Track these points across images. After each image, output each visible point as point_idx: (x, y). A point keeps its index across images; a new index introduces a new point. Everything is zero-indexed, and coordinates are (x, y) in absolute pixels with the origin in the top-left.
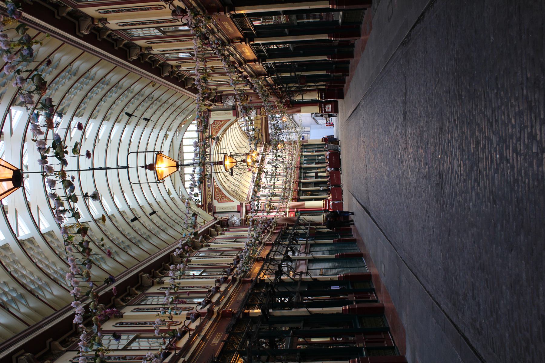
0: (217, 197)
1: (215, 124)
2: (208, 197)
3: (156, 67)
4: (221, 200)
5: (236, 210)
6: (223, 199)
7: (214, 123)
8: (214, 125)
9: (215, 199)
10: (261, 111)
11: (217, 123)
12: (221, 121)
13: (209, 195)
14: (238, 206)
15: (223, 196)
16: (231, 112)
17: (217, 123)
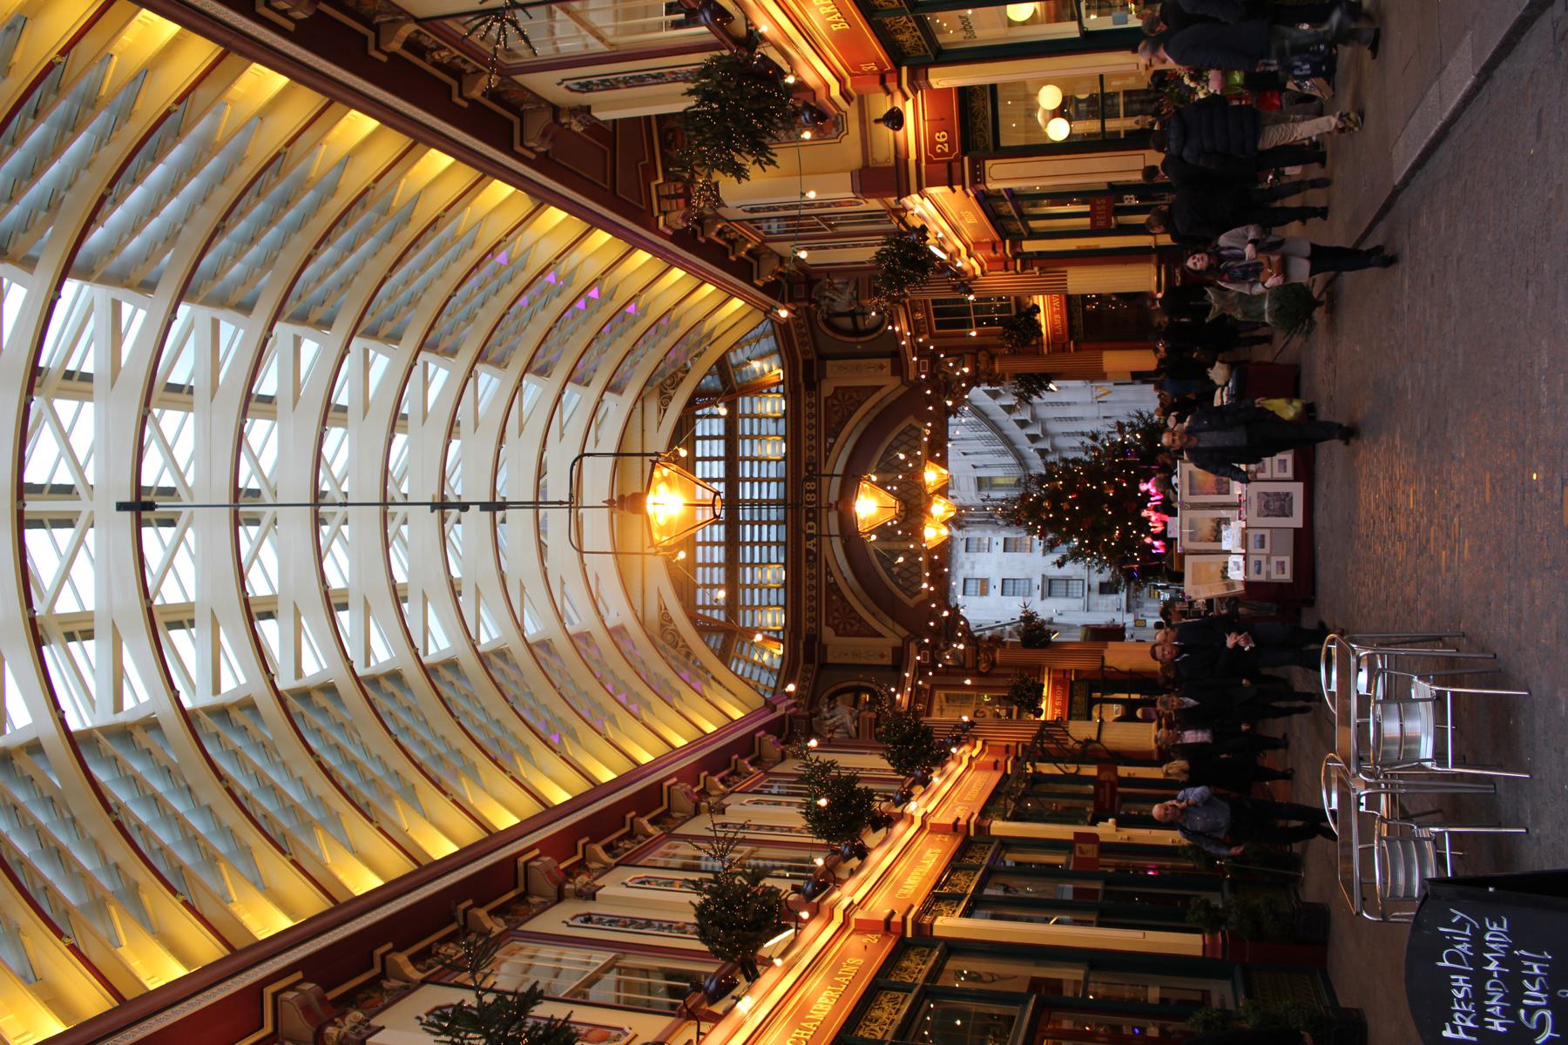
0: (834, 618)
1: (836, 398)
2: (804, 614)
3: (740, 259)
4: (845, 628)
5: (888, 661)
6: (852, 625)
7: (834, 396)
8: (836, 402)
9: (827, 624)
10: (977, 361)
11: (843, 395)
12: (857, 389)
13: (811, 609)
14: (895, 649)
15: (854, 618)
16: (887, 362)
17: (843, 395)
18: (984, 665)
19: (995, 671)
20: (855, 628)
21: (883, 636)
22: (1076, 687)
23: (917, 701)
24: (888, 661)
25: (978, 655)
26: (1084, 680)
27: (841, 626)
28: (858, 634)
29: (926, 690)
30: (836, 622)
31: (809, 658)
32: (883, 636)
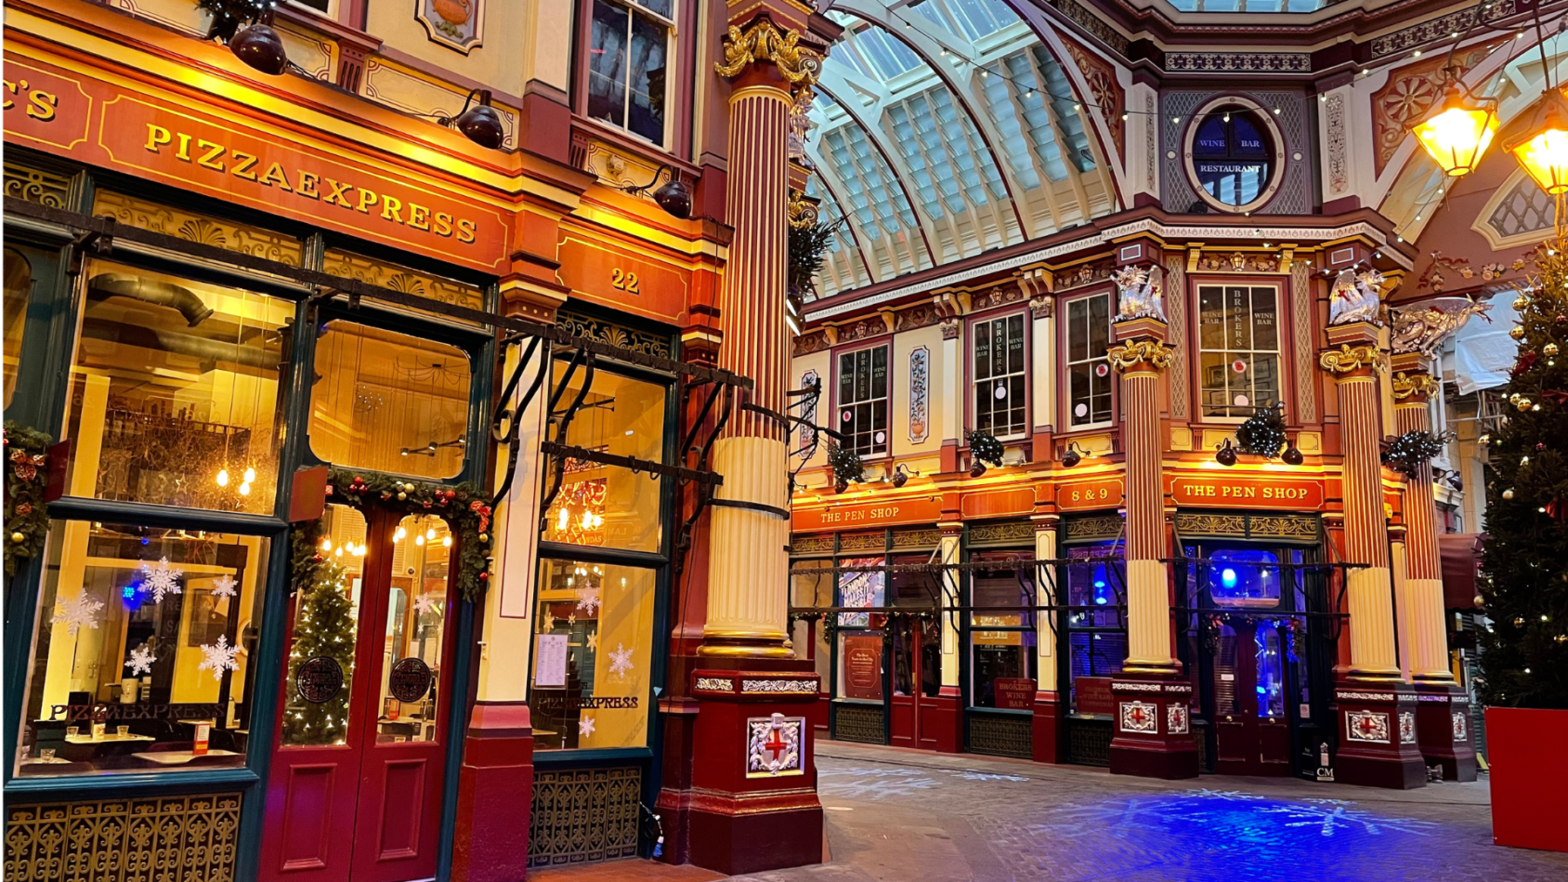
4: (1389, 105)
5: (1328, 196)
6: (1396, 116)
9: (1391, 72)
14: (1354, 199)
15: (1410, 117)
18: (1332, 359)
19: (1328, 381)
20: (1392, 124)
21: (1377, 176)
22: (1308, 521)
23: (1250, 257)
24: (1328, 196)
25: (1352, 345)
26: (1322, 534)
27: (1392, 99)
28: (1378, 130)
29: (1276, 269)
30: (1402, 88)
31: (1318, 60)
32: (1377, 176)
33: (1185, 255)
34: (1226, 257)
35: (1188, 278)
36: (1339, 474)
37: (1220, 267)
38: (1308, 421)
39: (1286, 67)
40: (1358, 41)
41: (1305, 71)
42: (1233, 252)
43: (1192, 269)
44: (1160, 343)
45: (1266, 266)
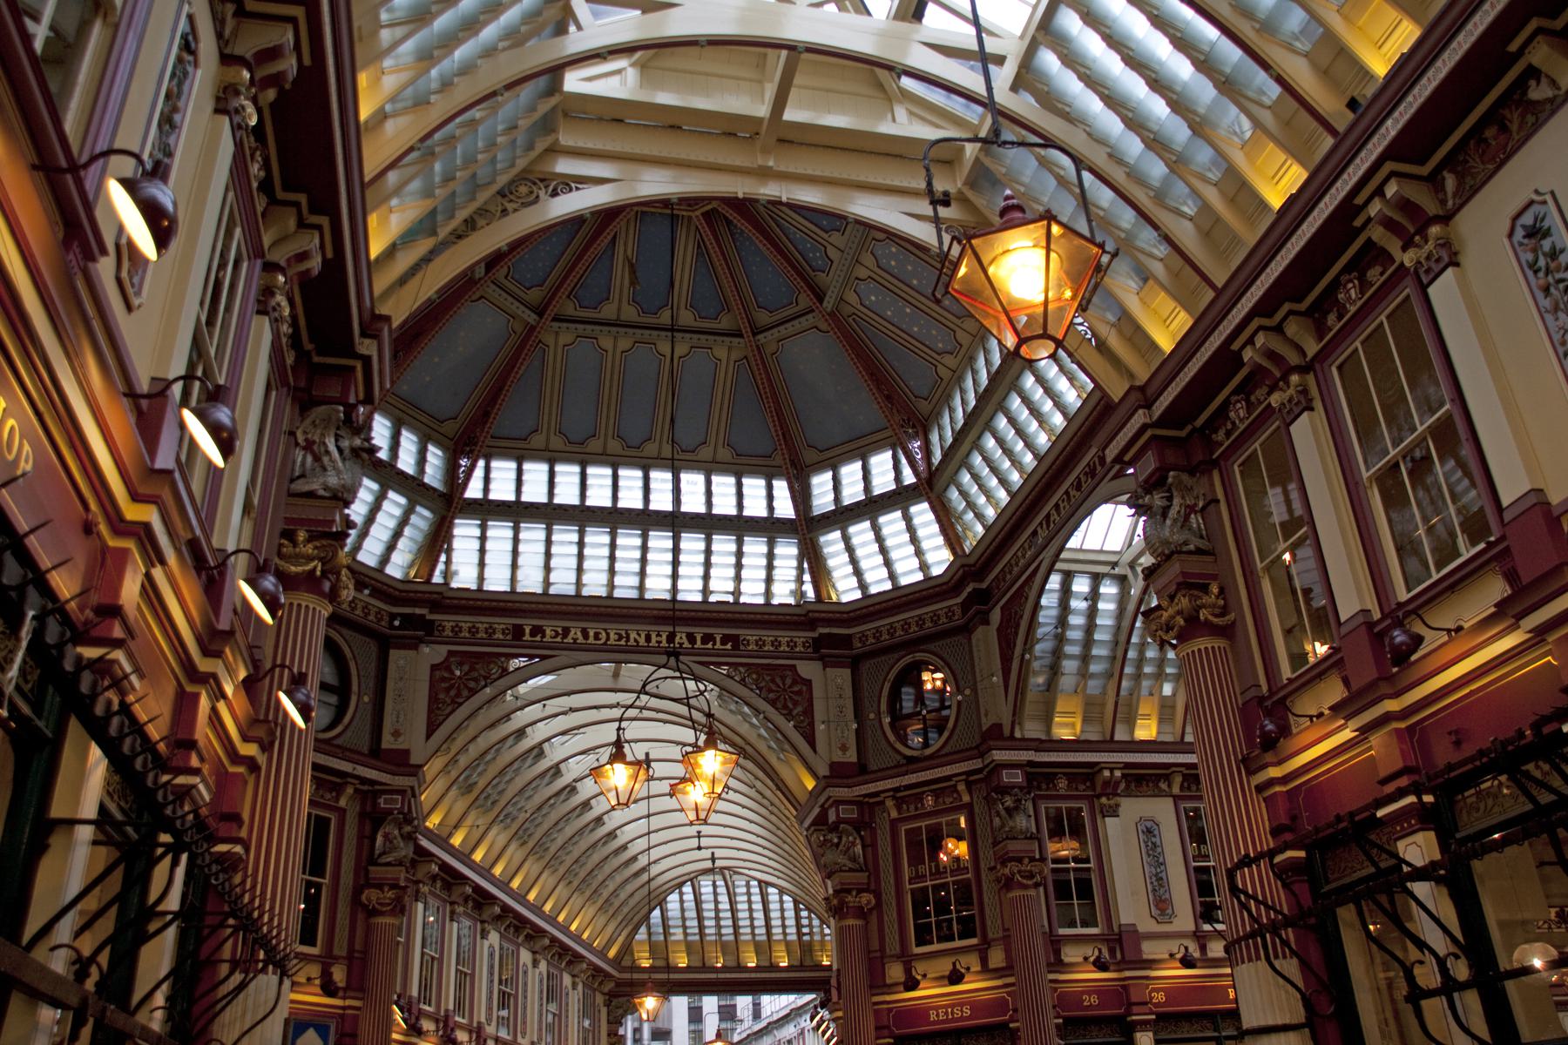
9: (1002, 608)
23: (937, 794)
31: (965, 606)
33: (882, 803)
34: (919, 798)
35: (894, 823)
36: (1012, 985)
37: (916, 809)
38: (996, 936)
39: (929, 624)
40: (984, 585)
41: (958, 620)
42: (924, 792)
43: (894, 814)
44: (854, 893)
45: (949, 800)
